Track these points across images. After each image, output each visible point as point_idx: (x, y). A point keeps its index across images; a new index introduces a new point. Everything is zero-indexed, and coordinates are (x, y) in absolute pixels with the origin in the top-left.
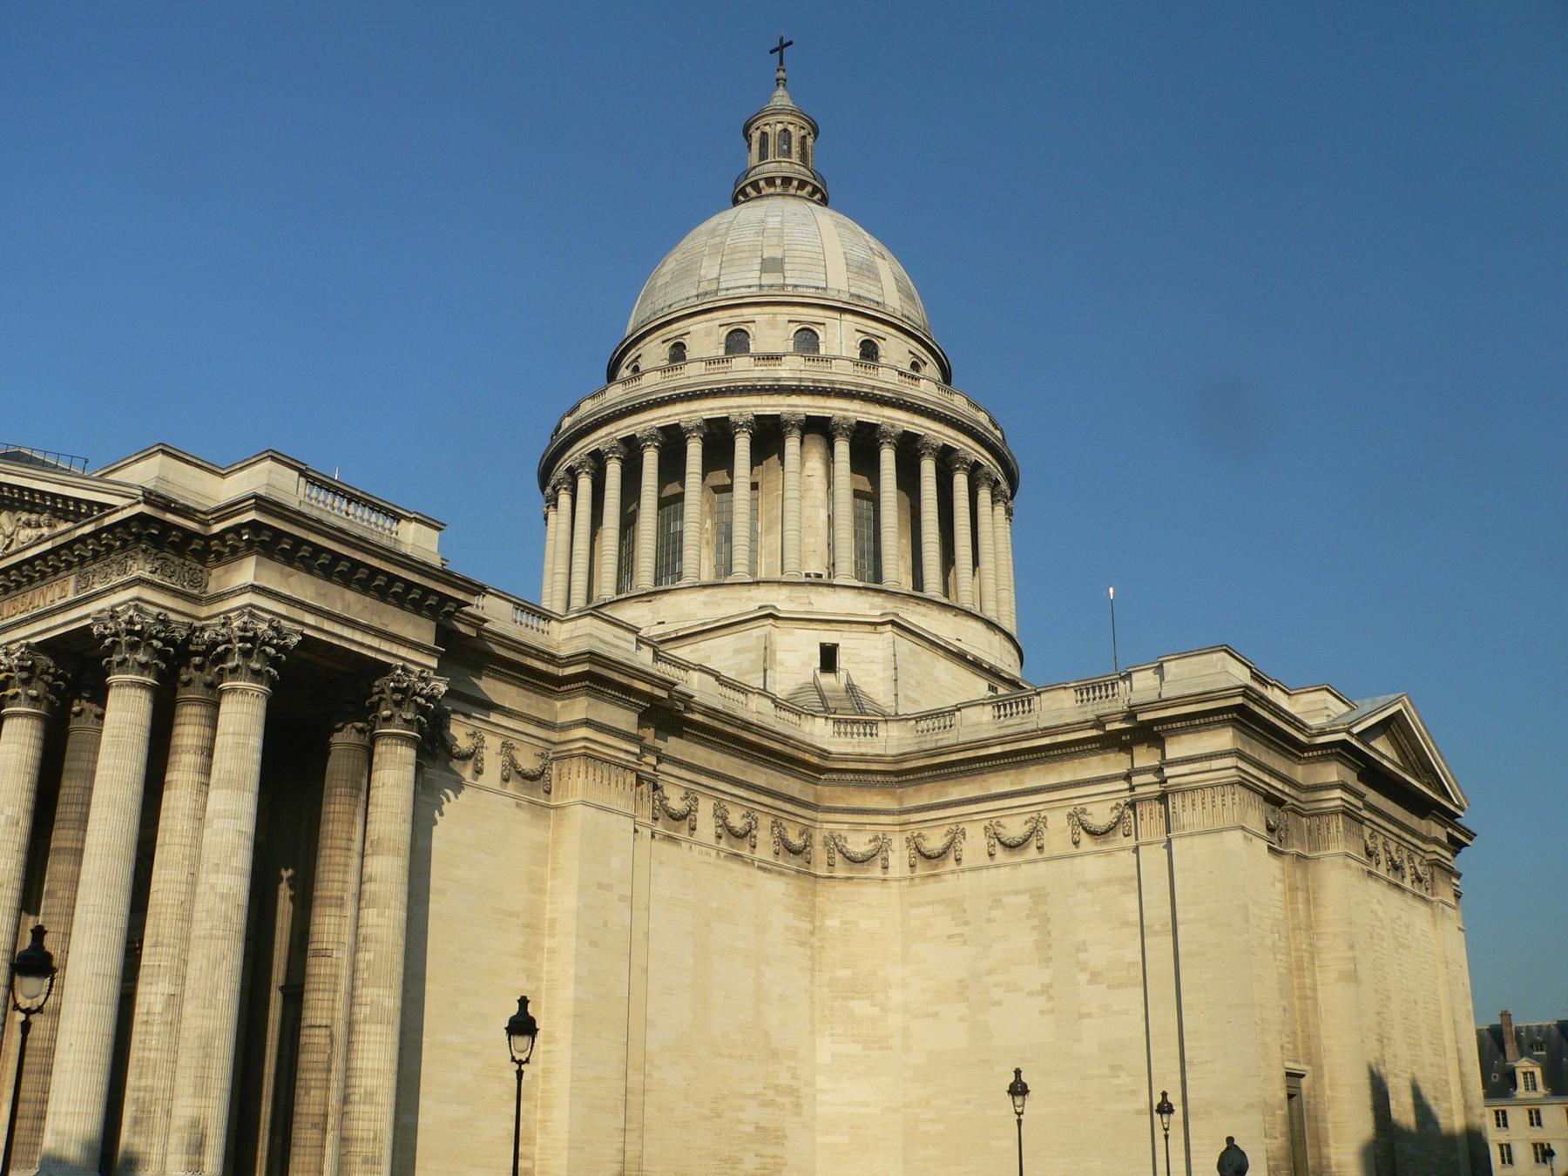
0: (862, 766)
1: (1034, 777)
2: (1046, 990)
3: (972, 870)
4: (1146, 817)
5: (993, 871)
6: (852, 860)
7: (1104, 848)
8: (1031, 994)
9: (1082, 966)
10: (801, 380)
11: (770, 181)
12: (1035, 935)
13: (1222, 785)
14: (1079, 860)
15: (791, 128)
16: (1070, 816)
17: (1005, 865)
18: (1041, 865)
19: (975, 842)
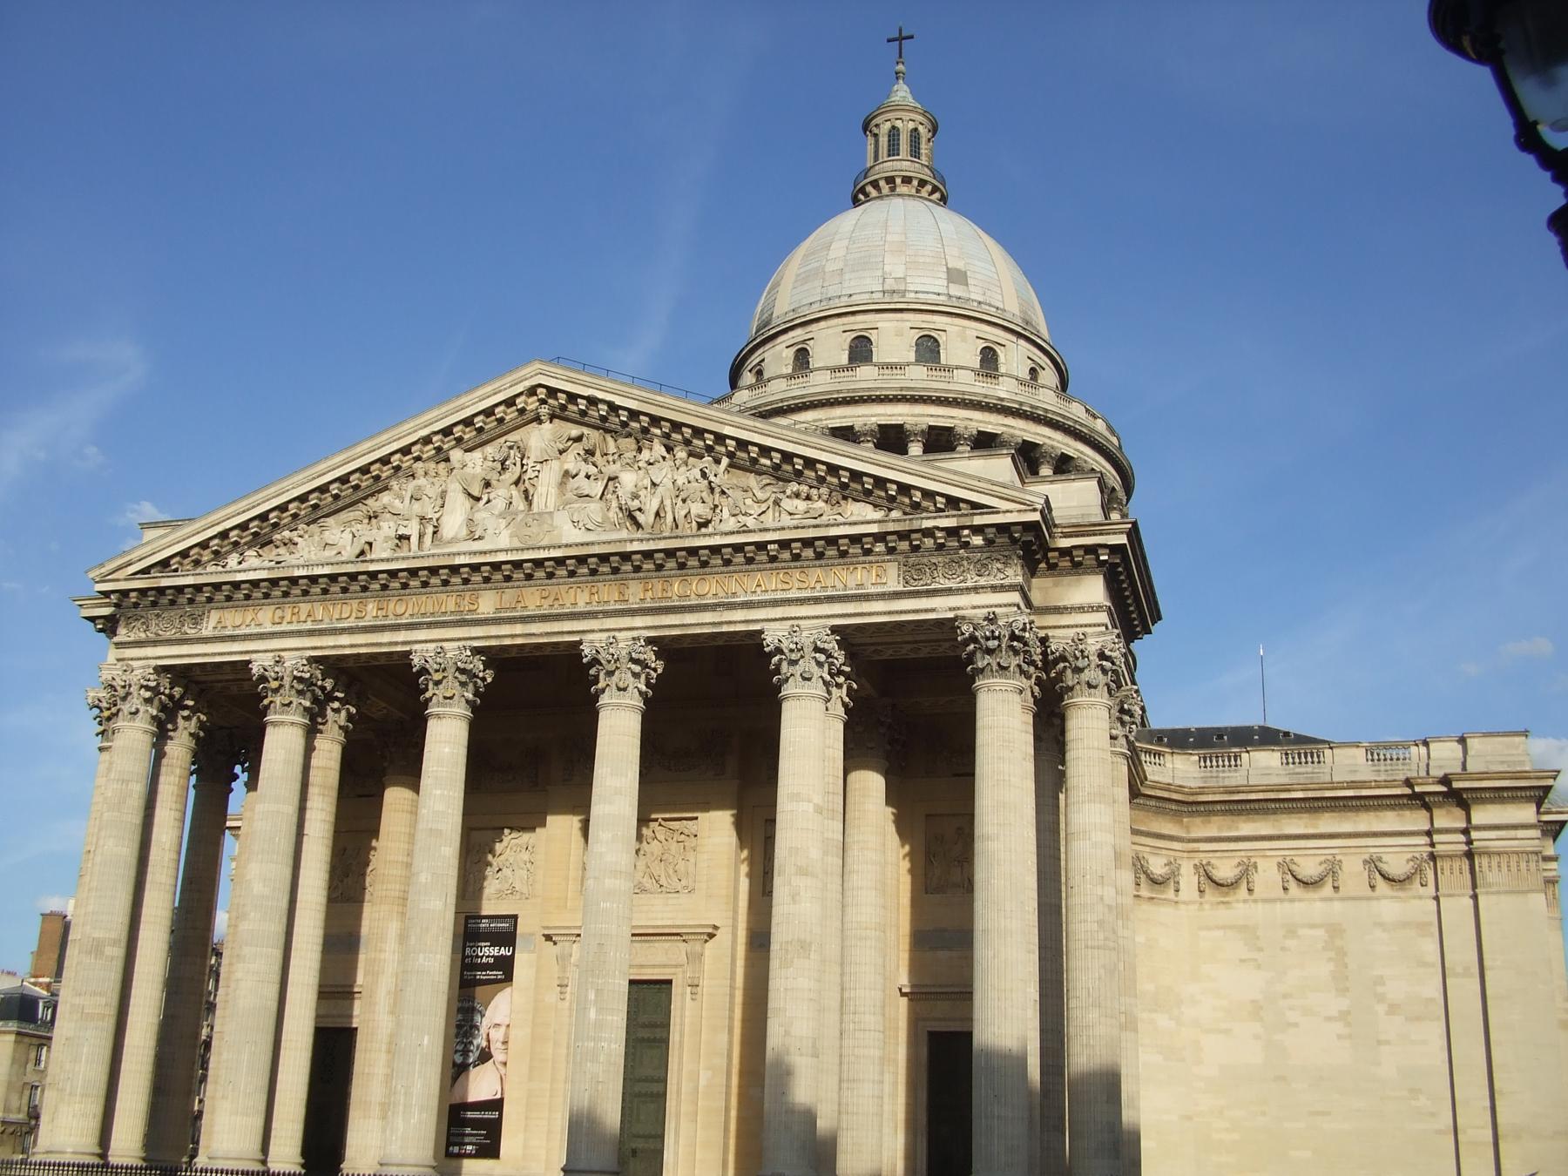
0: (1166, 794)
1: (1328, 823)
2: (1344, 1016)
3: (1265, 901)
4: (1447, 872)
5: (1286, 905)
6: (1155, 882)
7: (1400, 894)
8: (1329, 1019)
9: (1381, 998)
10: (1021, 404)
11: (907, 180)
12: (1331, 966)
13: (1527, 853)
14: (1374, 903)
15: (921, 128)
16: (1365, 862)
17: (1300, 900)
18: (1337, 905)
19: (1267, 874)
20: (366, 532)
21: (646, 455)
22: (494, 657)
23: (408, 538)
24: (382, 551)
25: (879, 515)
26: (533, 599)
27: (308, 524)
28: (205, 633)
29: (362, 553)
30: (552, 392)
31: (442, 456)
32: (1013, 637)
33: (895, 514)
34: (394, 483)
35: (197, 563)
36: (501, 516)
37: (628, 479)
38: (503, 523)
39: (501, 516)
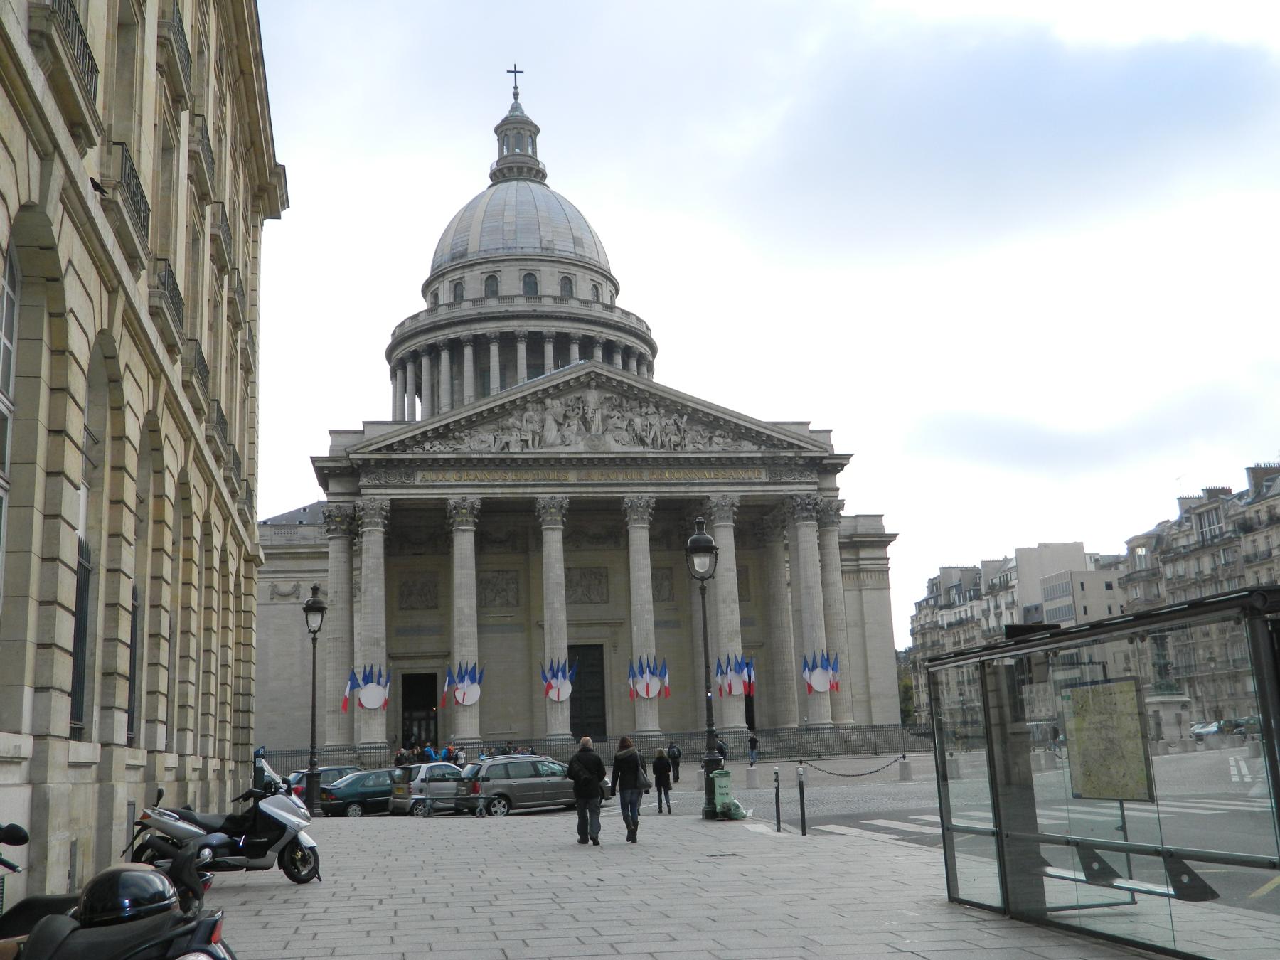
11: (530, 169)
20: (506, 438)
21: (644, 410)
22: (573, 501)
23: (526, 441)
24: (515, 448)
25: (755, 448)
26: (596, 476)
27: (471, 429)
28: (417, 482)
29: (503, 448)
30: (598, 375)
31: (541, 401)
32: (816, 504)
33: (763, 448)
34: (515, 413)
35: (407, 446)
36: (578, 434)
37: (638, 421)
38: (579, 438)
39: (578, 434)
